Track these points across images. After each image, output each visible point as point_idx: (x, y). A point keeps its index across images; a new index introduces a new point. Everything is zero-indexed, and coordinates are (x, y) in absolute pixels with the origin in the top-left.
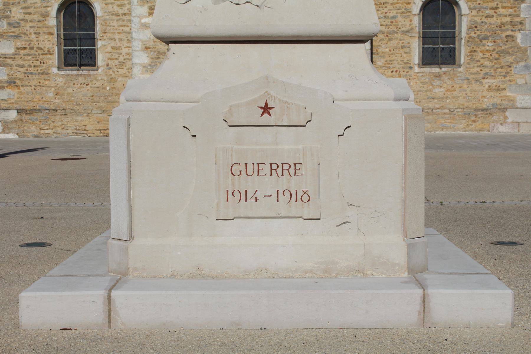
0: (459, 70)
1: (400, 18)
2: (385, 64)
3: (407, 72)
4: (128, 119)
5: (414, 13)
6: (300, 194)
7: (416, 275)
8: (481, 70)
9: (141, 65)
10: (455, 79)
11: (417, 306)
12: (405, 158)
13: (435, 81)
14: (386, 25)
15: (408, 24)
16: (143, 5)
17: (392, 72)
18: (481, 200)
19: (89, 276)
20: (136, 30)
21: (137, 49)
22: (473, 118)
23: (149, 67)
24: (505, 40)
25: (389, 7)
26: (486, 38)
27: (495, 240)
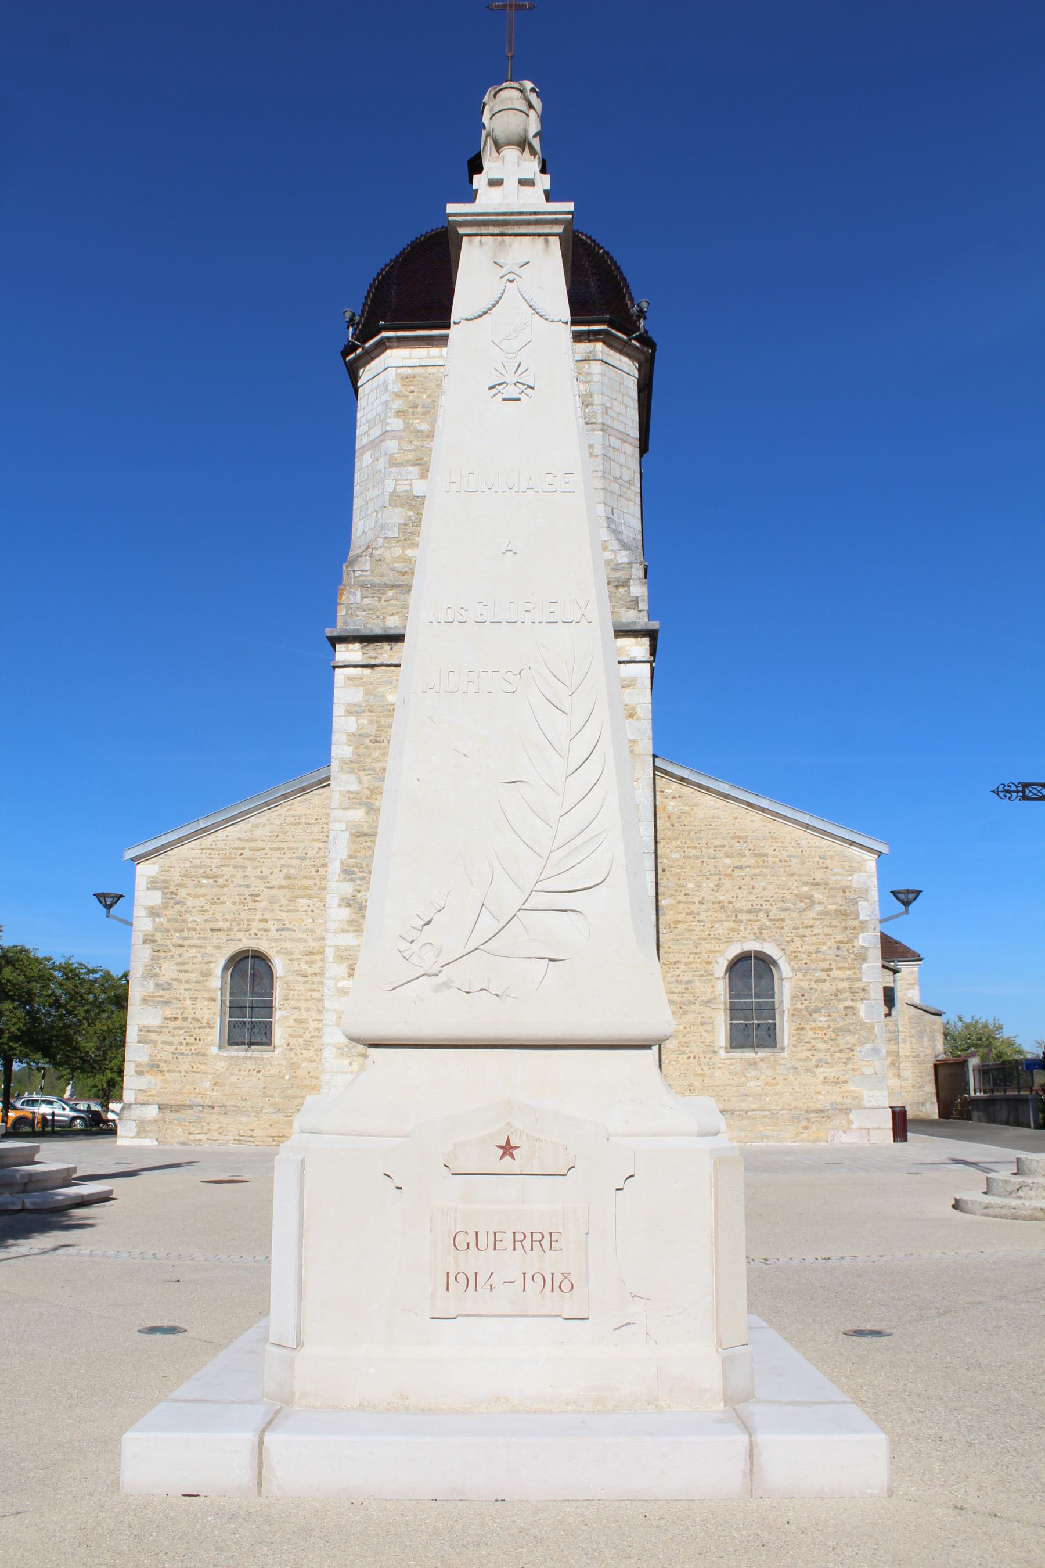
0: (782, 1055)
1: (697, 983)
4: (303, 1161)
7: (736, 1407)
12: (716, 1223)
15: (709, 992)
18: (824, 1256)
19: (233, 1402)
22: (804, 1123)
24: (844, 1013)
25: (682, 967)
26: (817, 1010)
27: (851, 1326)
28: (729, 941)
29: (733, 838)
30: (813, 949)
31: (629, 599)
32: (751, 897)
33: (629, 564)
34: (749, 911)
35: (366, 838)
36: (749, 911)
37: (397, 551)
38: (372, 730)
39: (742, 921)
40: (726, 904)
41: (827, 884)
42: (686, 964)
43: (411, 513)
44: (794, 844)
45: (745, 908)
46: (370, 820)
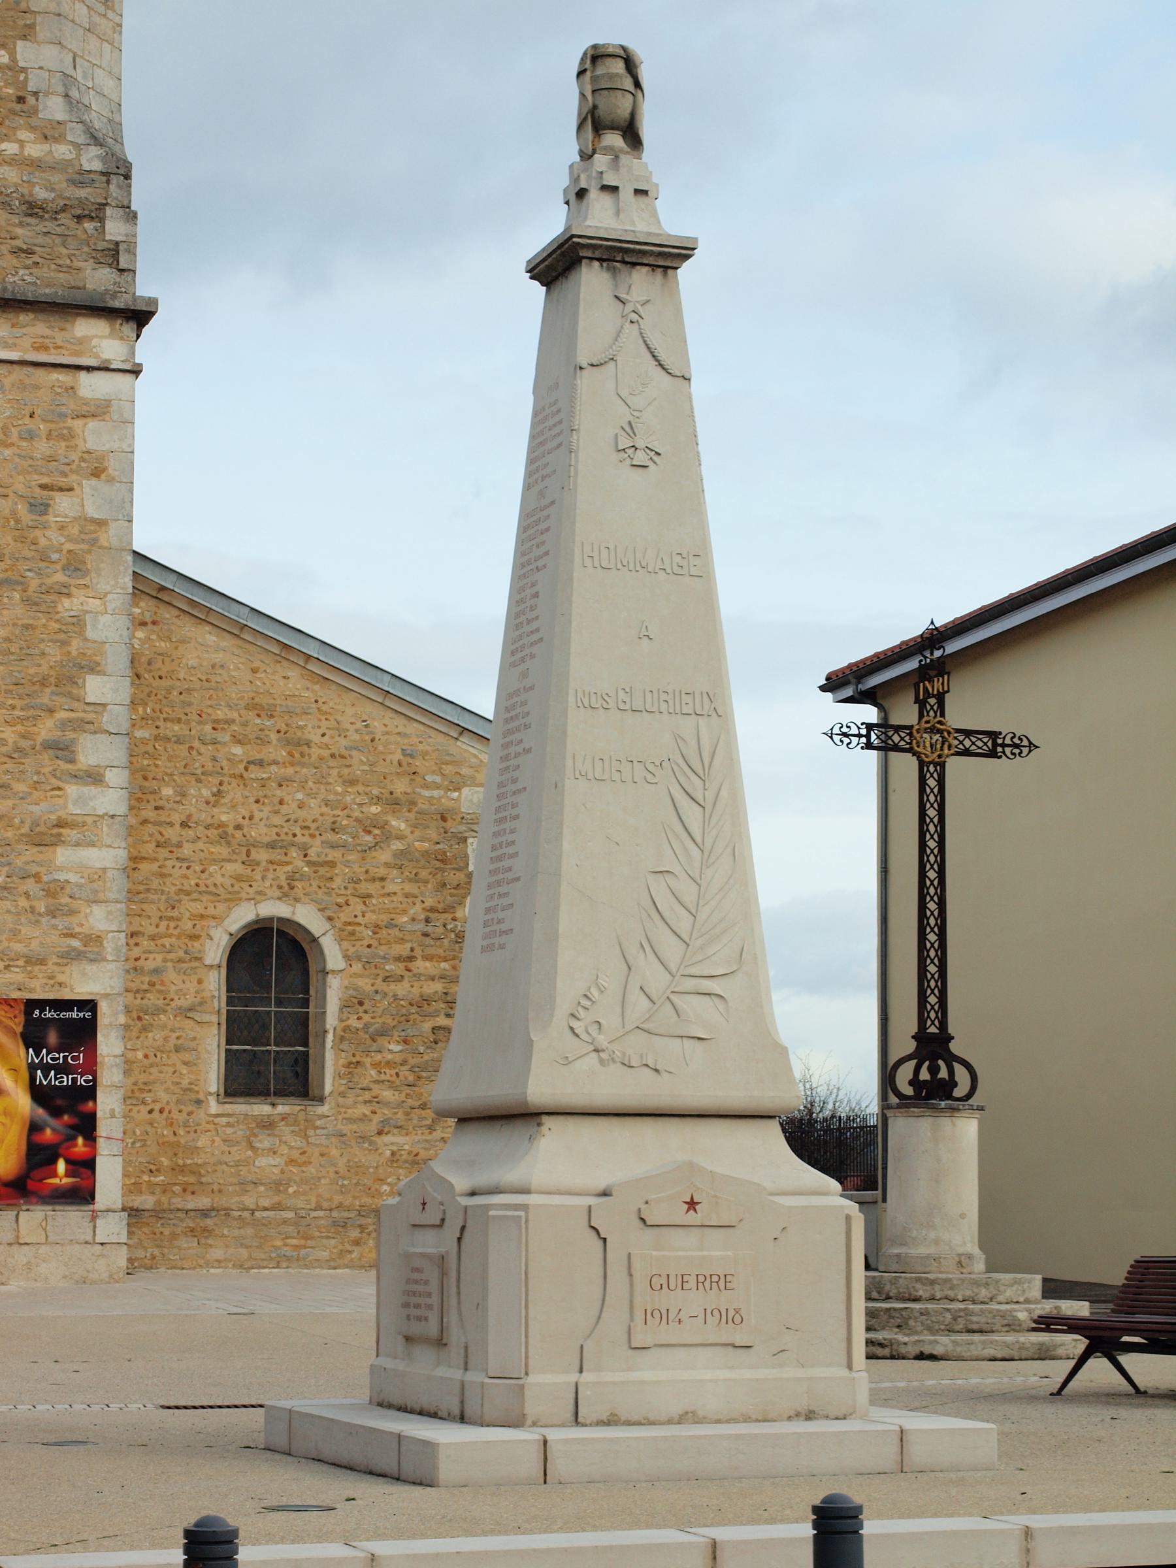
1: (171, 975)
2: (133, 1091)
3: (190, 1114)
5: (208, 962)
8: (374, 1113)
10: (311, 1132)
13: (260, 1137)
14: (137, 991)
15: (192, 991)
17: (150, 1112)
22: (354, 1234)
25: (145, 943)
26: (383, 1033)
28: (234, 899)
29: (247, 708)
30: (385, 918)
31: (101, 245)
32: (277, 820)
33: (103, 174)
34: (272, 846)
36: (272, 846)
39: (258, 864)
40: (230, 830)
41: (413, 803)
42: (152, 938)
44: (359, 725)
45: (266, 840)
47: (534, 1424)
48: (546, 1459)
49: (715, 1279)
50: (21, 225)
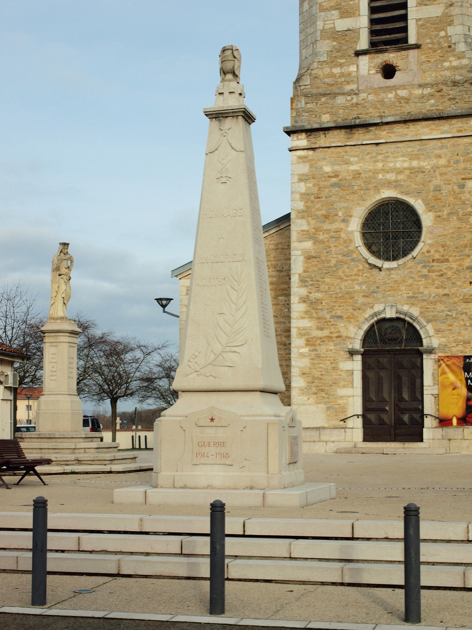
6: (225, 454)
9: (298, 388)
11: (261, 499)
16: (301, 338)
20: (295, 359)
21: (296, 375)
23: (305, 390)
35: (314, 259)
37: (327, 70)
38: (315, 190)
43: (335, 43)
46: (316, 248)
47: (161, 487)
48: (146, 497)
49: (220, 443)
50: (451, 90)
